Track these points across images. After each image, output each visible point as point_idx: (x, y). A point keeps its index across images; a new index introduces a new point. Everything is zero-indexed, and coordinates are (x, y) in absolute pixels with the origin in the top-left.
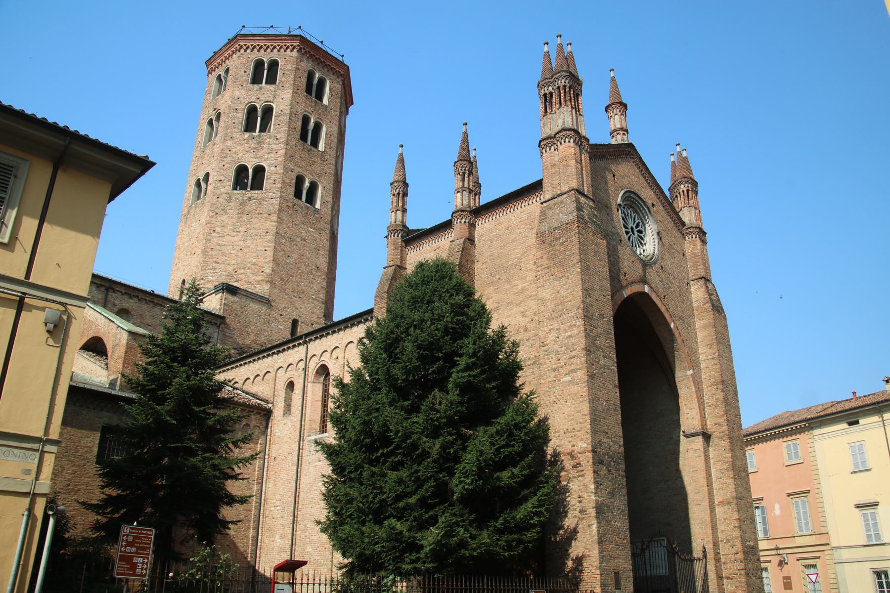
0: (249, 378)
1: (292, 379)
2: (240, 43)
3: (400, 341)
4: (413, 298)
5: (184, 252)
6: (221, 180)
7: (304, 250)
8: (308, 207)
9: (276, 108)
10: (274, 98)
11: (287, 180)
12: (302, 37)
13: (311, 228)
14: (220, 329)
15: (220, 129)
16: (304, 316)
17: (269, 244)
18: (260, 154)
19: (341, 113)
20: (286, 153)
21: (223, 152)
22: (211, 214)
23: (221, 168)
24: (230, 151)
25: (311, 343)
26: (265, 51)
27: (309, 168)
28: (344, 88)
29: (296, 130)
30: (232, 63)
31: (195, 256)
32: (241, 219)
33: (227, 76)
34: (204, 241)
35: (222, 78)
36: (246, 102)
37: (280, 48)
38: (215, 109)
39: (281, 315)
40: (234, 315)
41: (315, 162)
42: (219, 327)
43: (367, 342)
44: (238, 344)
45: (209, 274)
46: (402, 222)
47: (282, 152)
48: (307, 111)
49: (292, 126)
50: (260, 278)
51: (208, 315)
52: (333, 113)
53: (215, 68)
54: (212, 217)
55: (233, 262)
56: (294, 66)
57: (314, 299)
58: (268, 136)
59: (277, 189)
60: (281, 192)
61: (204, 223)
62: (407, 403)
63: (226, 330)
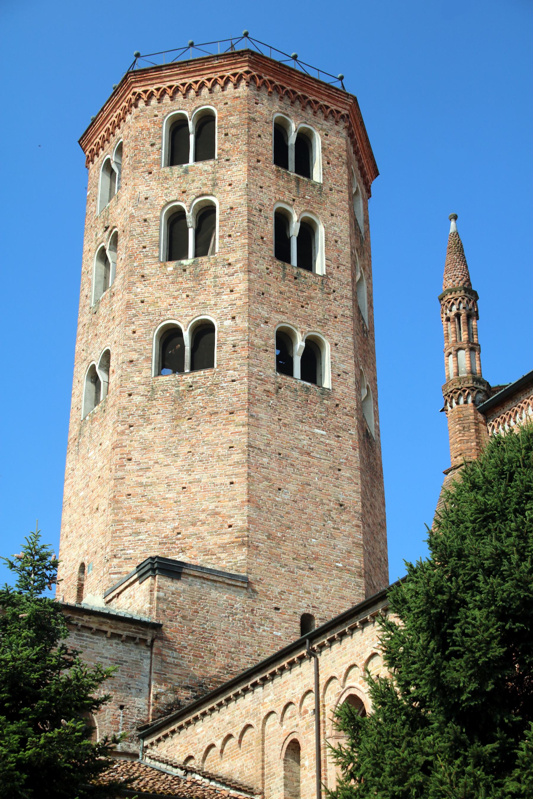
0: (212, 746)
1: (295, 736)
2: (135, 90)
3: (459, 606)
4: (482, 512)
5: (80, 510)
6: (131, 361)
7: (309, 474)
8: (308, 388)
9: (221, 204)
10: (215, 185)
11: (258, 341)
12: (253, 53)
13: (318, 428)
14: (154, 651)
15: (120, 264)
16: (324, 606)
17: (237, 471)
18: (201, 298)
19: (352, 197)
20: (249, 289)
21: (129, 306)
22: (120, 428)
23: (129, 338)
24: (142, 302)
25: (324, 653)
26: (185, 96)
27: (299, 311)
28: (354, 144)
29: (264, 242)
30: (126, 133)
31: (98, 514)
32: (178, 430)
33: (121, 160)
34: (112, 483)
35: (114, 166)
36: (163, 203)
37: (213, 85)
38: (107, 228)
39: (277, 609)
40: (179, 619)
41: (310, 298)
42: (151, 647)
43: (399, 622)
44: (194, 677)
45: (127, 544)
46: (472, 372)
47: (242, 287)
48: (283, 202)
49: (256, 234)
50: (226, 539)
51: (128, 625)
52: (335, 197)
53: (98, 150)
54: (123, 433)
55: (172, 514)
56: (244, 116)
57: (341, 569)
58: (212, 261)
59: (241, 361)
60: (249, 365)
61: (110, 447)
62: (489, 747)
63: (165, 651)
